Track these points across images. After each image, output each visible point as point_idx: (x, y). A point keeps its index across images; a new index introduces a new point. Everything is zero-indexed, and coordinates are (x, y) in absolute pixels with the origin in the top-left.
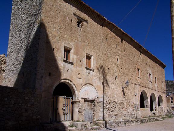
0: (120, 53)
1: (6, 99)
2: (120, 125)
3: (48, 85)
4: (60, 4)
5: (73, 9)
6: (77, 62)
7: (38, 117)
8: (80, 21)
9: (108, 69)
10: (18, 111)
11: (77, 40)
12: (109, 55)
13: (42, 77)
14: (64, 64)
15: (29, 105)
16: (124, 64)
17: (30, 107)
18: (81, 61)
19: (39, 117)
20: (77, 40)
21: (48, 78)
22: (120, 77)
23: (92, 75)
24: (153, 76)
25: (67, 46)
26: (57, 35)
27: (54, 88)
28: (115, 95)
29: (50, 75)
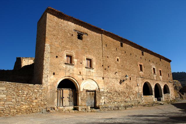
0: (120, 54)
1: (20, 92)
2: (120, 108)
3: (53, 81)
4: (61, 25)
5: (72, 26)
6: (77, 64)
7: (45, 103)
8: (80, 36)
9: (108, 67)
10: (29, 99)
11: (78, 48)
12: (109, 56)
13: (48, 76)
14: (66, 67)
15: (38, 95)
16: (124, 62)
17: (38, 96)
18: (81, 63)
19: (46, 103)
20: (78, 48)
21: (53, 76)
22: (120, 72)
23: (93, 72)
24: (158, 70)
25: (68, 53)
26: (58, 46)
27: (58, 83)
28: (115, 86)
29: (54, 74)
